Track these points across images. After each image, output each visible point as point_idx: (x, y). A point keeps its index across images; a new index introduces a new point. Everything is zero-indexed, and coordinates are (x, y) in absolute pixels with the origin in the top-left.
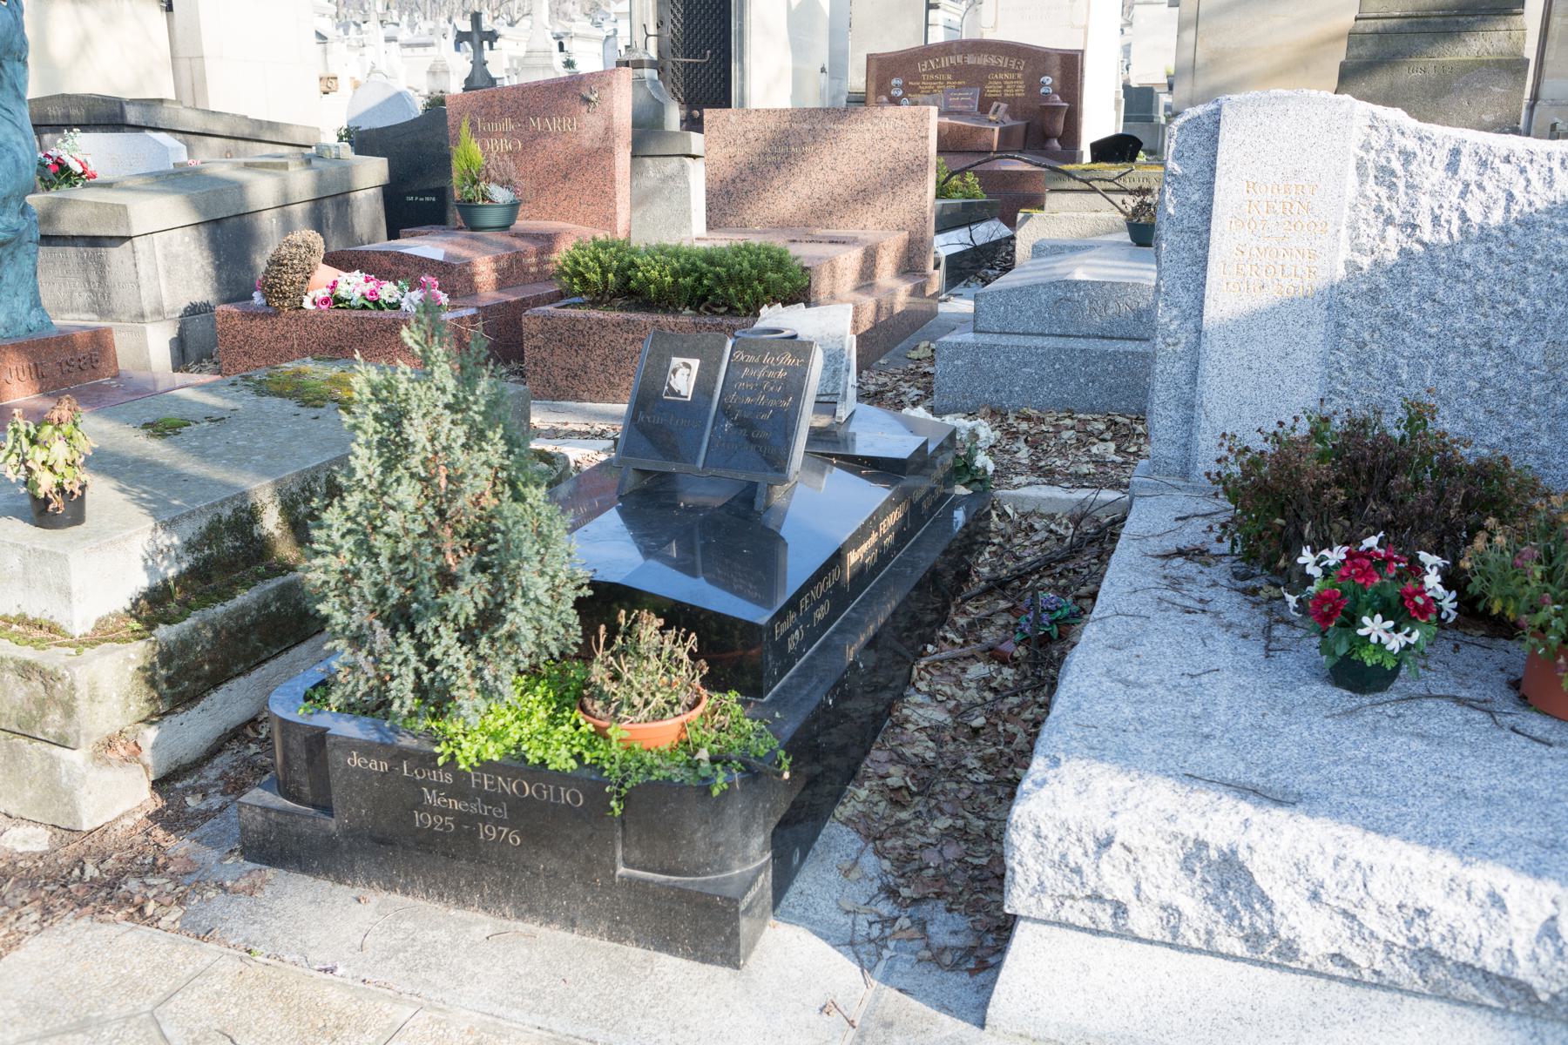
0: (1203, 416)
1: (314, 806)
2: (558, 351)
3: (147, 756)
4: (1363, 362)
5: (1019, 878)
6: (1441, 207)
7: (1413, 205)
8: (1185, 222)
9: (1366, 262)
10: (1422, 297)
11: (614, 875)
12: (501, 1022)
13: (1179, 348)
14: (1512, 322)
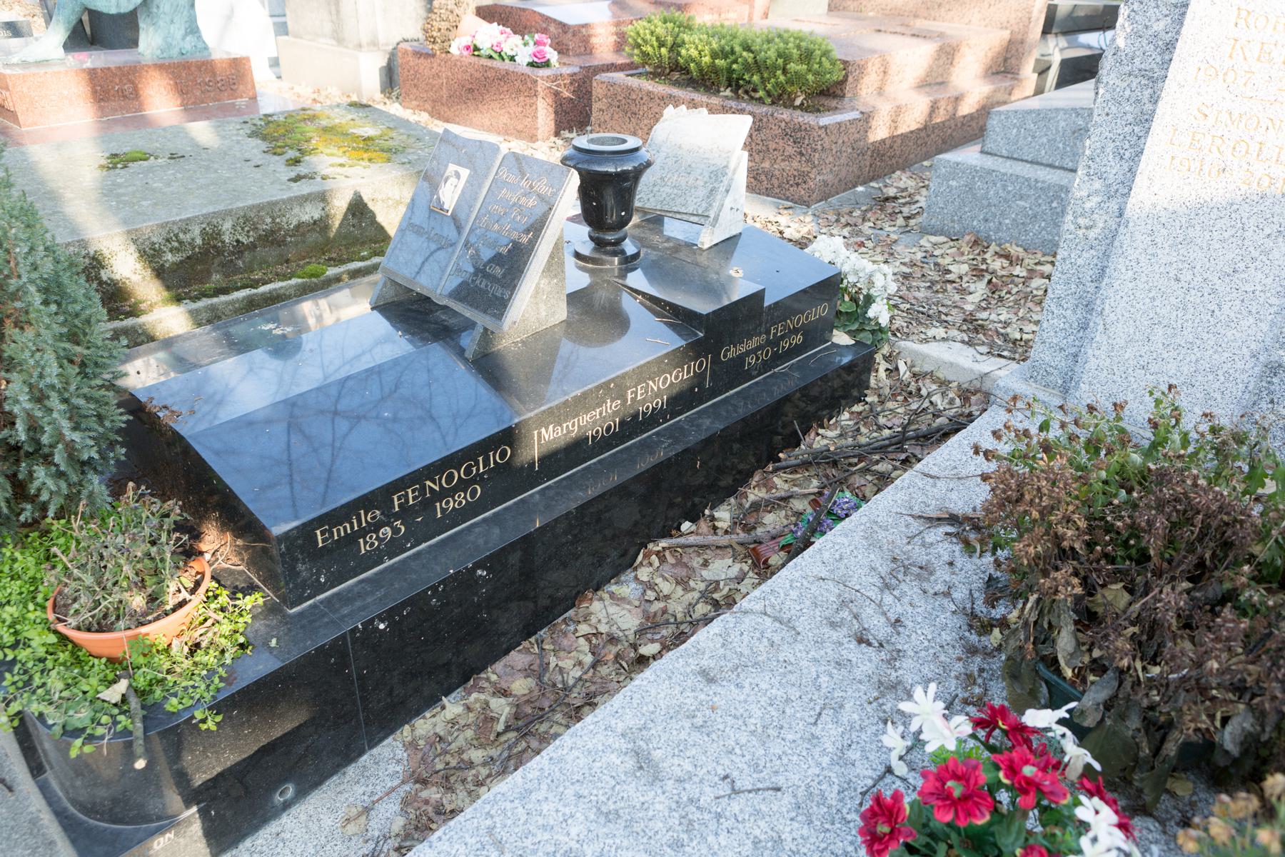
0: (1101, 328)
2: (616, 116)
8: (1137, 61)
13: (1092, 234)
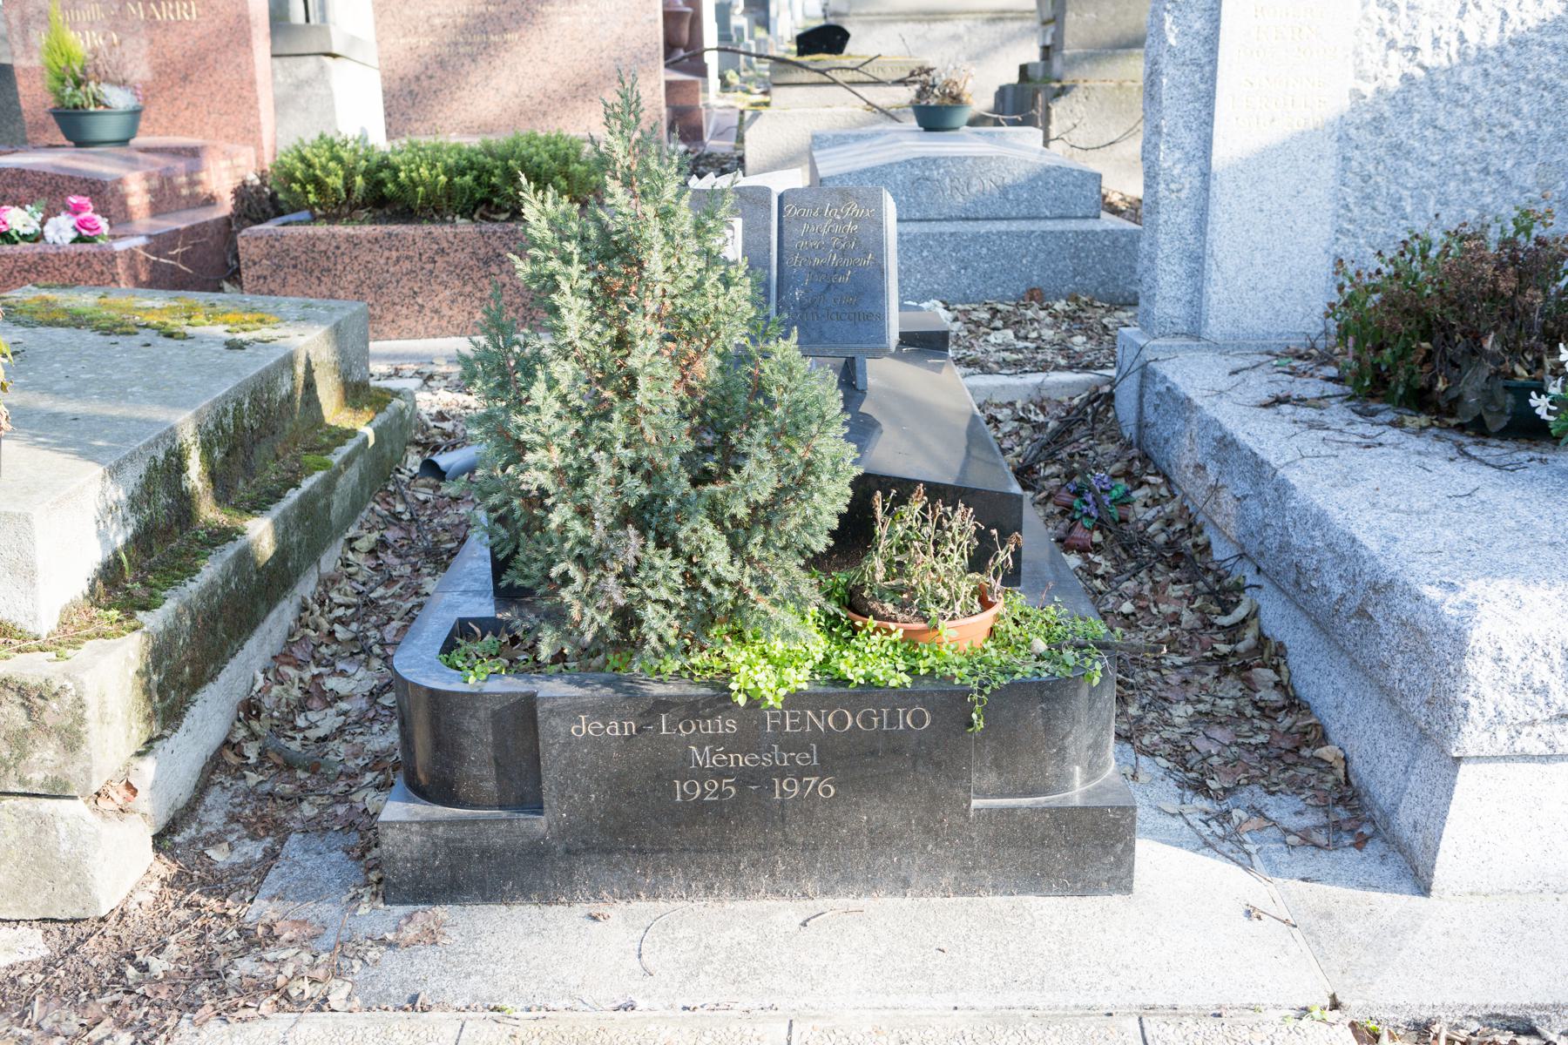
0: (1214, 267)
1: (501, 807)
2: (292, 280)
3: (144, 802)
4: (1368, 197)
5: (1473, 713)
6: (1441, 28)
7: (1415, 27)
8: (1187, 53)
9: (1369, 89)
10: (1424, 124)
11: (967, 809)
12: (905, 1013)
13: (1183, 195)
14: (1508, 145)
